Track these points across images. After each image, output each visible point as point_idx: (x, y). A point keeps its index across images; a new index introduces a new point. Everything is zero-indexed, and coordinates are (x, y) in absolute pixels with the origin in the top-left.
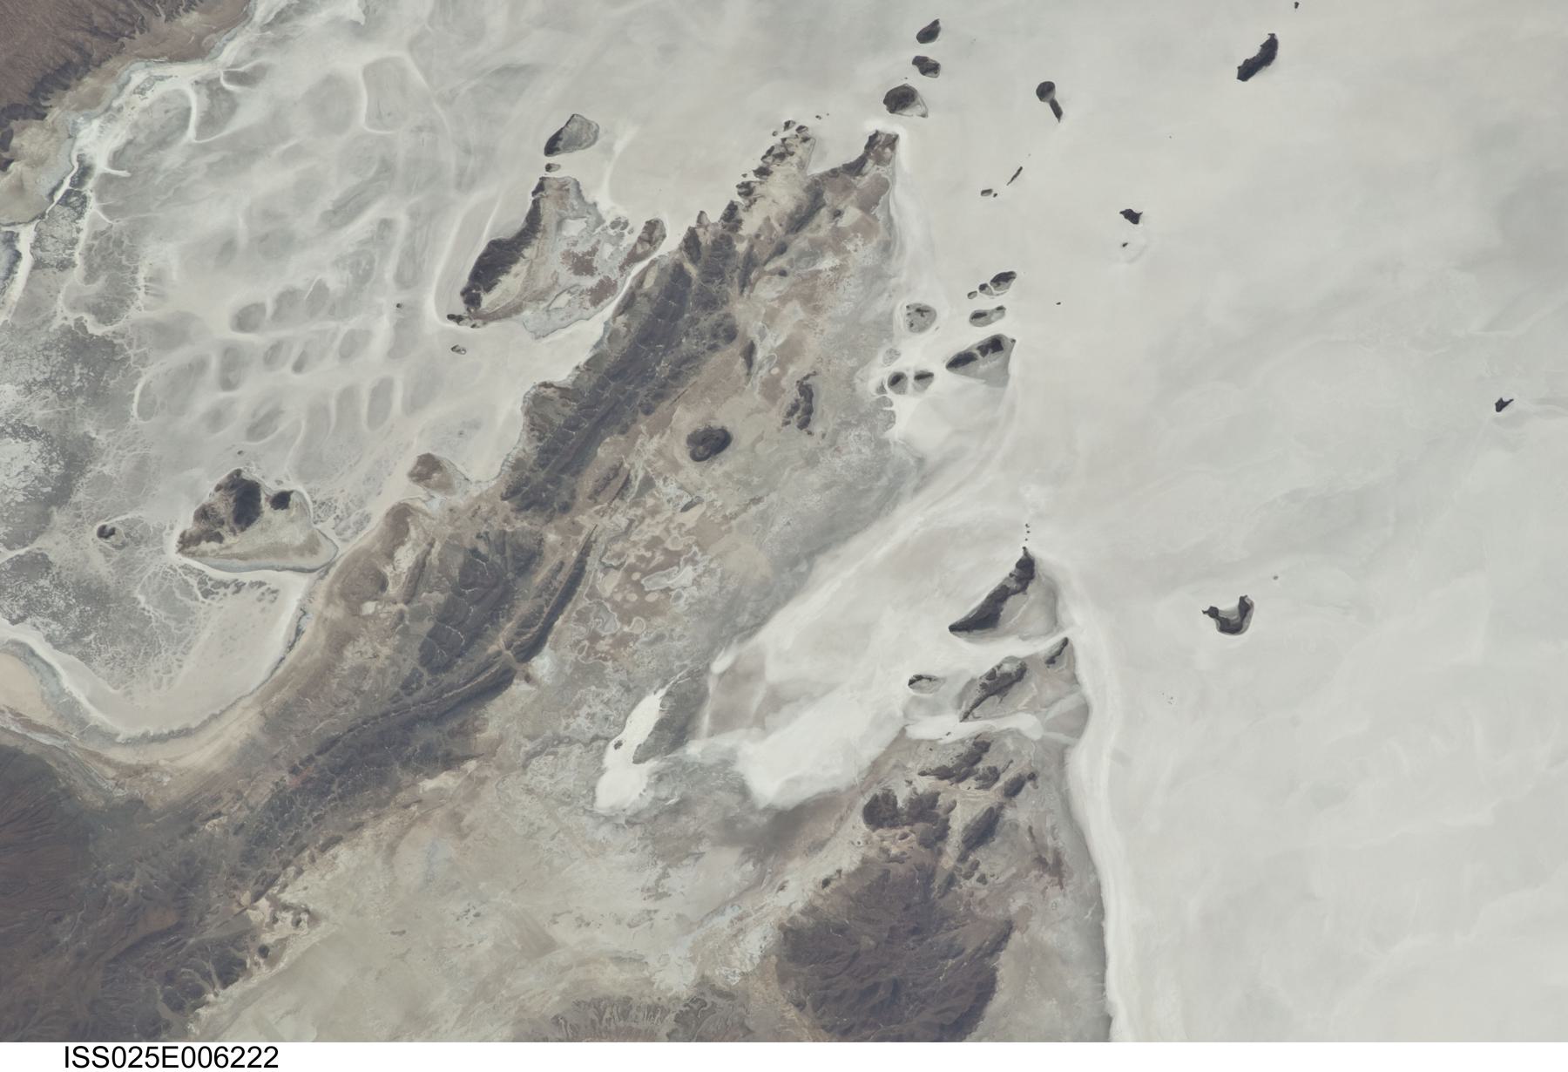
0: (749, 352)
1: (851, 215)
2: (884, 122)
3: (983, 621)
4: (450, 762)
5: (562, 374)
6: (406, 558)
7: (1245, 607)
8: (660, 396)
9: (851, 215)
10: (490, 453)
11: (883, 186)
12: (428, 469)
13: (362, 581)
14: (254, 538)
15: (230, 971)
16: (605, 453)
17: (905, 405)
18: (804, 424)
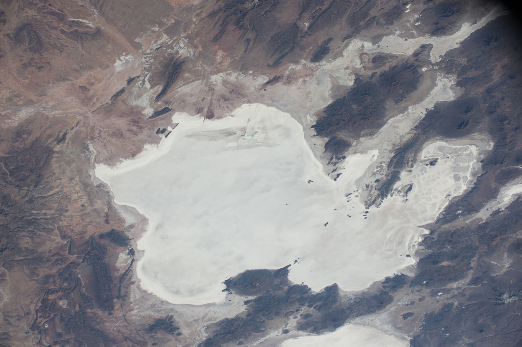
0: (376, 189)
1: (368, 202)
2: (367, 210)
3: (338, 175)
4: (397, 149)
5: (397, 182)
6: (410, 164)
7: (309, 183)
8: (385, 184)
9: (368, 202)
10: (403, 174)
11: (365, 205)
12: (410, 171)
13: (414, 161)
14: (430, 161)
15: (416, 127)
16: (389, 178)
17: (355, 189)
18: (367, 185)
